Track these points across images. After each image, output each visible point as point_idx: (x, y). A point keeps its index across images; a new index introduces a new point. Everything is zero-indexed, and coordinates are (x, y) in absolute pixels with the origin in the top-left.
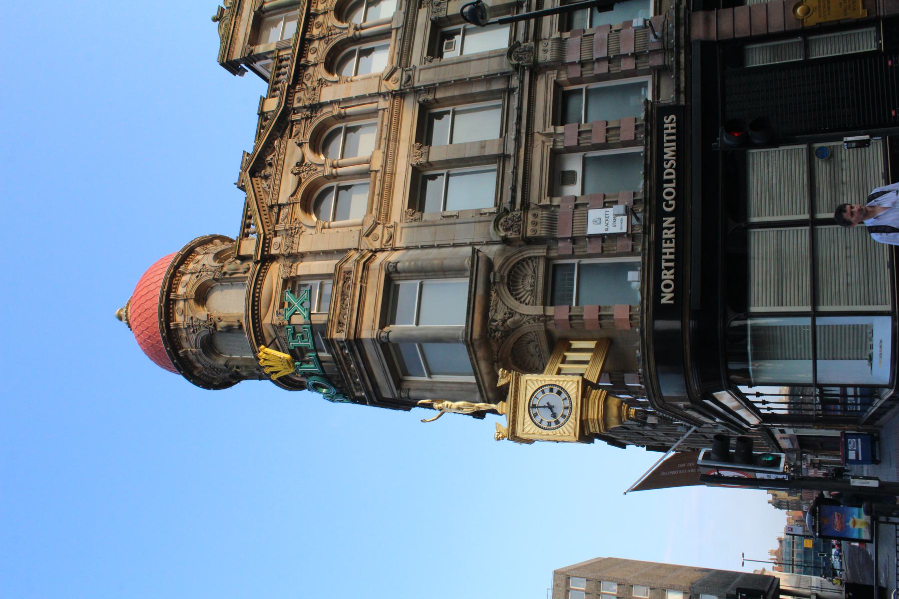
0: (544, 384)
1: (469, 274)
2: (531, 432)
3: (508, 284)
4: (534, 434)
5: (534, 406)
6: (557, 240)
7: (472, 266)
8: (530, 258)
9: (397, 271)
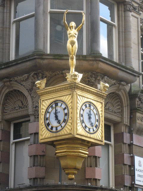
0: (101, 115)
1: (123, 64)
2: (78, 101)
3: (113, 93)
4: (77, 103)
5: (90, 106)
6: (130, 132)
7: (130, 70)
8: (122, 111)
9: (125, 11)
